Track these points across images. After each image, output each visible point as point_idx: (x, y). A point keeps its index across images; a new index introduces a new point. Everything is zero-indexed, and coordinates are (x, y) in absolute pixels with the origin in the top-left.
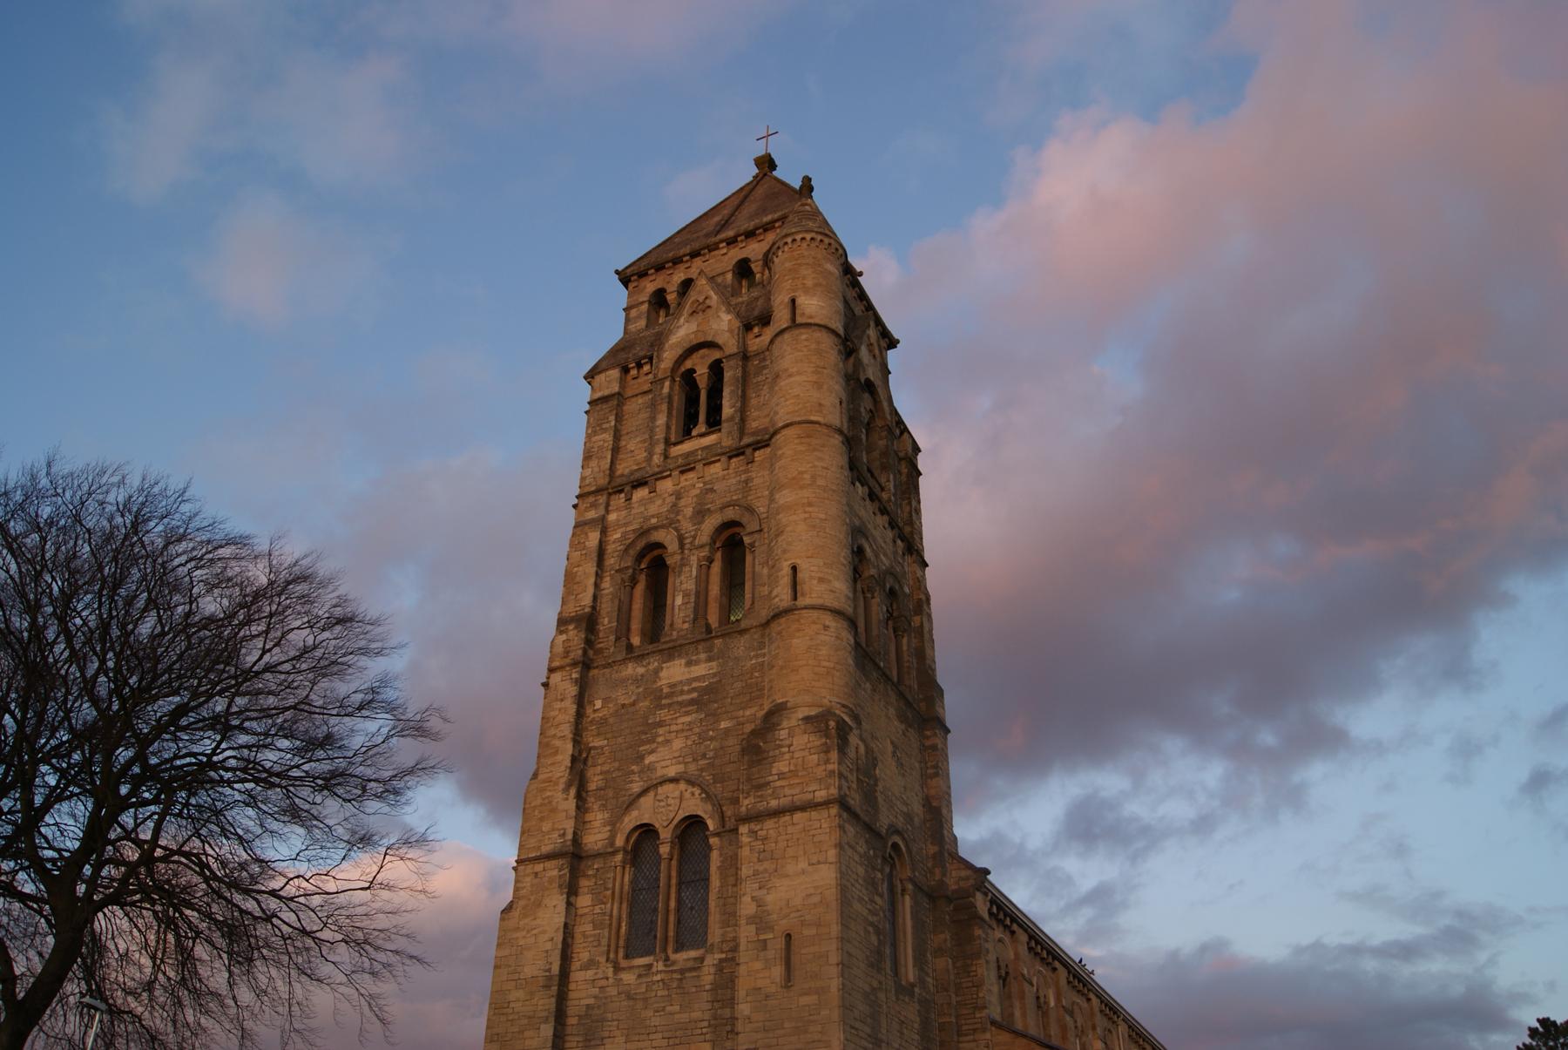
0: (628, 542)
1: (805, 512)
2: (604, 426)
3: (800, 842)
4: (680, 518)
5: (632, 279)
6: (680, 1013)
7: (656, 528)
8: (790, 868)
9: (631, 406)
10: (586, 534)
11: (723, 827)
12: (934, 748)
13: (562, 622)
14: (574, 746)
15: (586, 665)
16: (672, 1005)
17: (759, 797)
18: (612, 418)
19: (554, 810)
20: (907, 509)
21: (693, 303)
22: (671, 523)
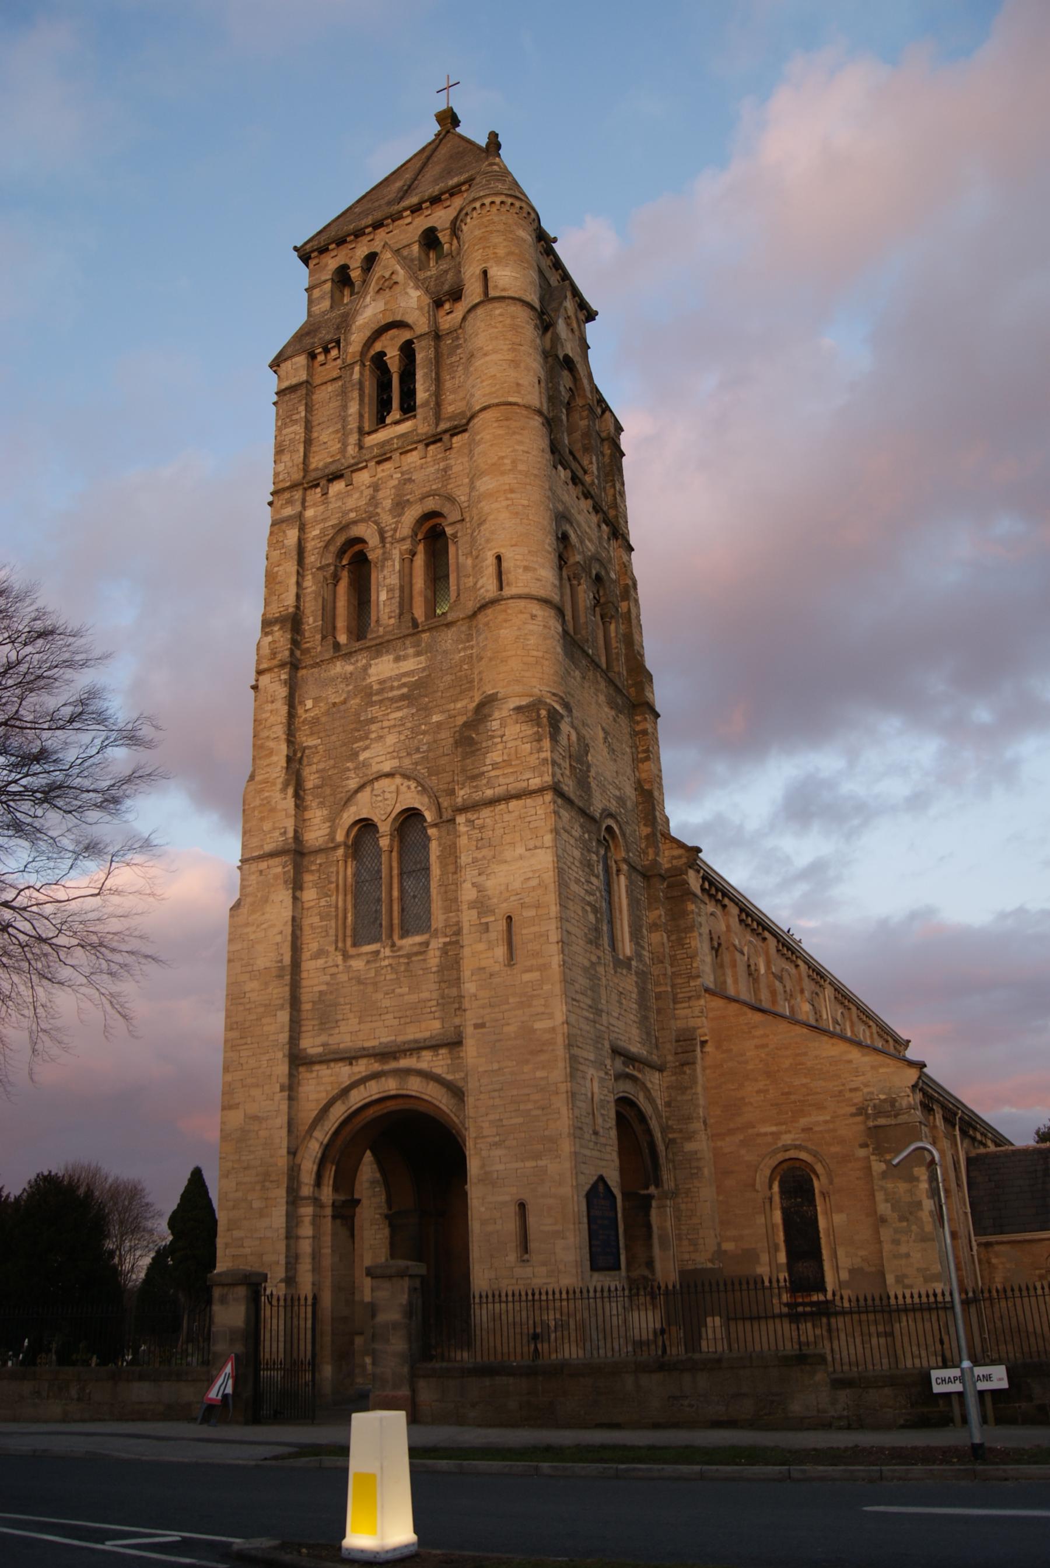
0: (327, 538)
1: (507, 499)
2: (295, 417)
3: (517, 828)
4: (379, 510)
5: (313, 255)
6: (409, 994)
7: (355, 522)
8: (508, 855)
9: (321, 395)
10: (284, 532)
11: (441, 818)
12: (645, 732)
13: (267, 624)
14: (288, 747)
15: (294, 665)
16: (401, 987)
17: (474, 787)
18: (302, 408)
19: (273, 810)
20: (612, 491)
21: (379, 279)
22: (370, 517)
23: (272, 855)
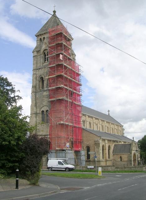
13: (32, 88)
22: (43, 75)
23: (34, 114)
